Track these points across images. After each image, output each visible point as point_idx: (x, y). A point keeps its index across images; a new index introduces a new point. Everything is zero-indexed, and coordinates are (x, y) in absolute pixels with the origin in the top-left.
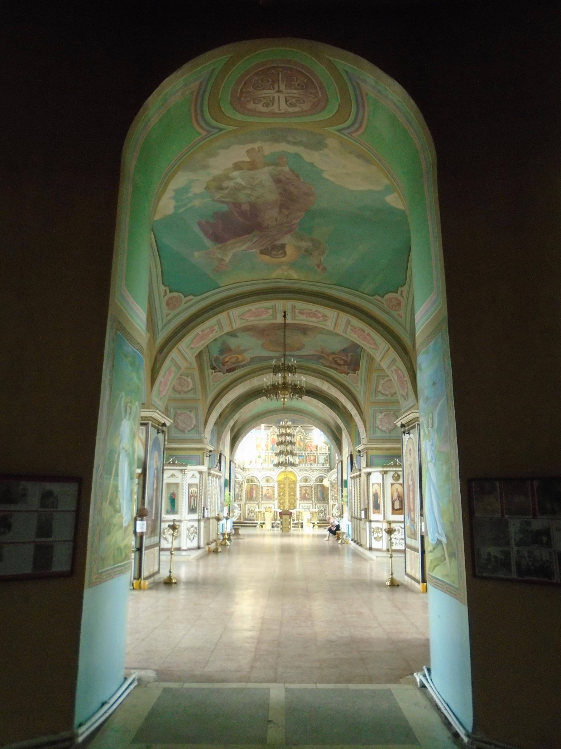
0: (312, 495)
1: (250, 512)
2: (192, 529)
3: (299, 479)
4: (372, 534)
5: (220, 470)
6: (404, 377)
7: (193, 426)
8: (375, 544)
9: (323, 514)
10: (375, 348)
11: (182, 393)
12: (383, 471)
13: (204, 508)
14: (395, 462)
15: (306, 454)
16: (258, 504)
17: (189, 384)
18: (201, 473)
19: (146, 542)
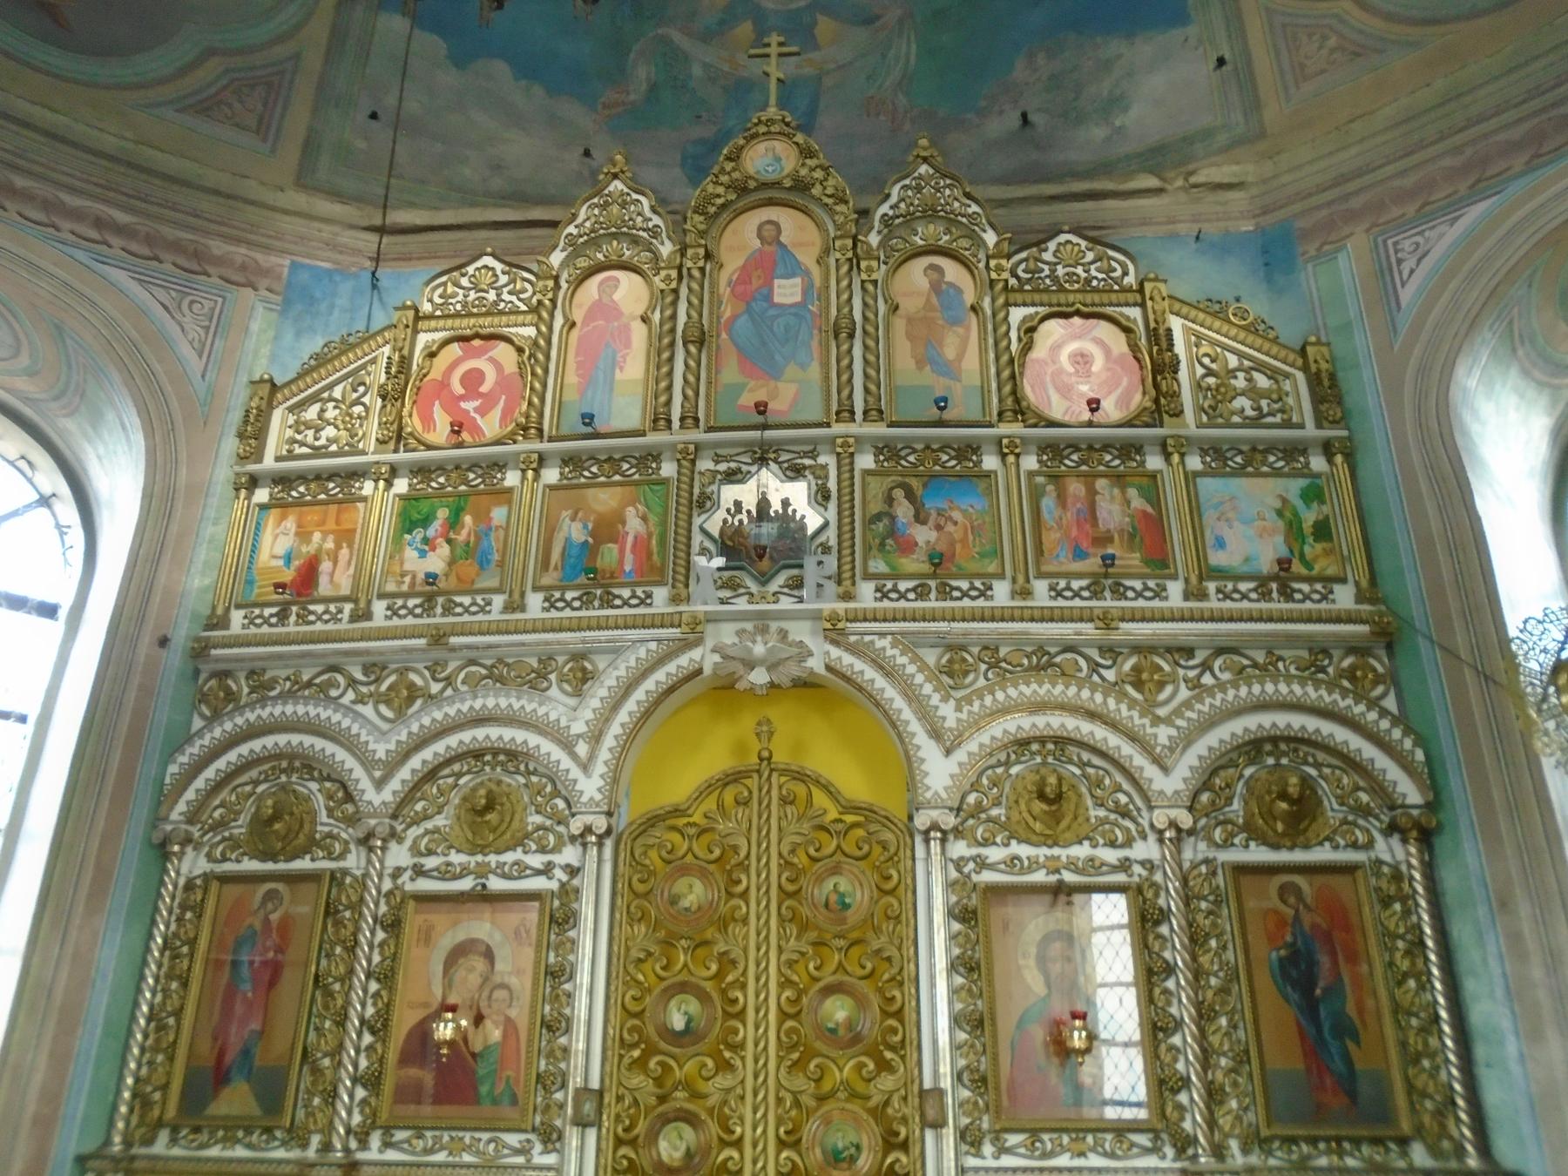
15: (1030, 462)
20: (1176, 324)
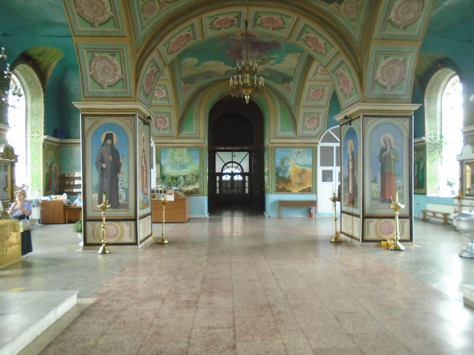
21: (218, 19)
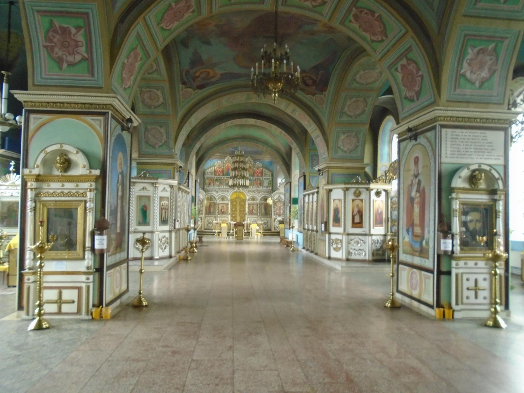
0: (257, 210)
1: (209, 223)
2: (163, 240)
3: (248, 198)
4: (331, 245)
5: (188, 186)
6: (418, 69)
7: (163, 141)
8: (334, 254)
9: (266, 225)
10: (380, 39)
11: (152, 107)
12: (345, 188)
13: (175, 220)
14: (358, 179)
16: (215, 217)
17: (159, 98)
18: (172, 187)
19: (108, 260)
20: (264, 169)
21: (312, 5)
